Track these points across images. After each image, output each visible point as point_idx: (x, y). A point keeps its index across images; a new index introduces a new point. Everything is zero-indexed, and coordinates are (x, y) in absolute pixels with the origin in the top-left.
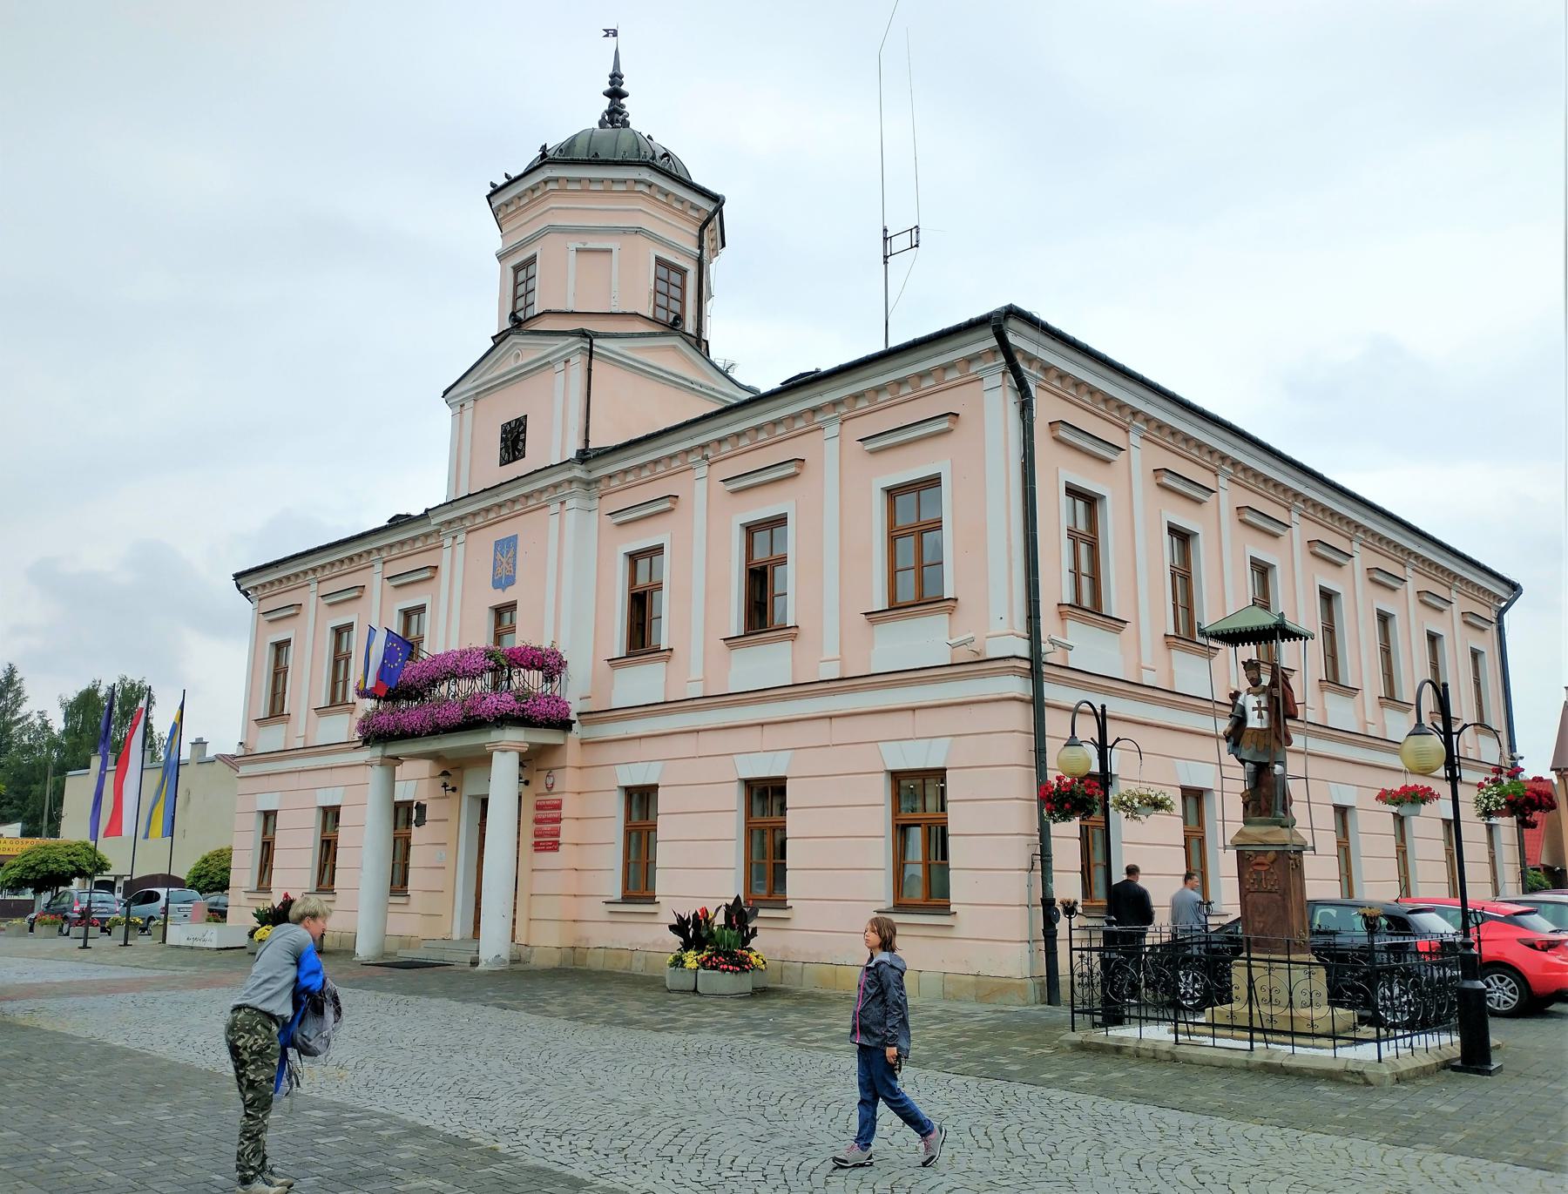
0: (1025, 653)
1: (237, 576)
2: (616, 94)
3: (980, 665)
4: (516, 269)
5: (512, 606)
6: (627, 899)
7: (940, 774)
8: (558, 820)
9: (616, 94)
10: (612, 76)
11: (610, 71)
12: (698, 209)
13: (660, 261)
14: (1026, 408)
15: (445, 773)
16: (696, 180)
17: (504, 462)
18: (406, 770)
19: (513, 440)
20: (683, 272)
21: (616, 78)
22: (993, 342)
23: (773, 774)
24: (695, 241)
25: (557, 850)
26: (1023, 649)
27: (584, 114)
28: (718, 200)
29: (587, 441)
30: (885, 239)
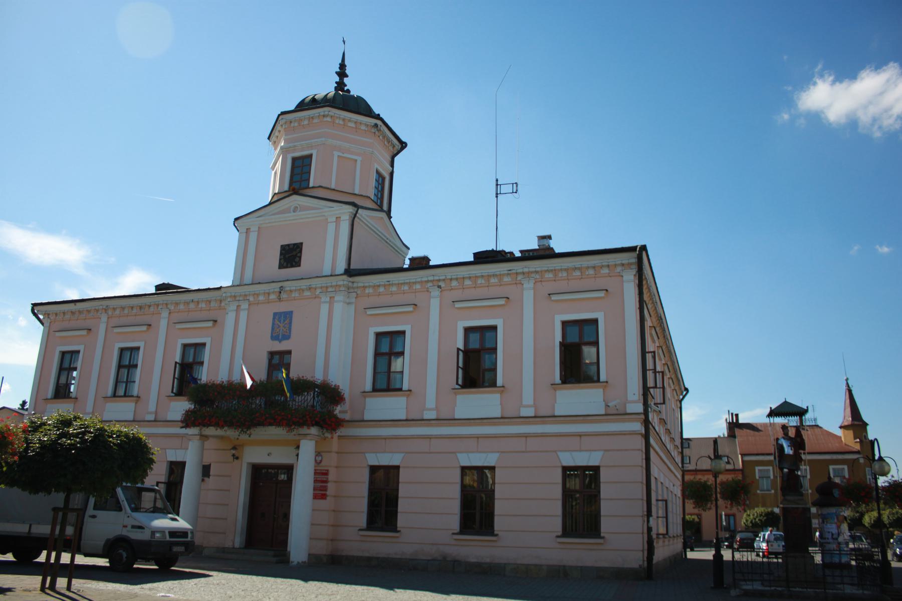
1: (34, 305)
3: (622, 415)
4: (294, 160)
8: (326, 482)
11: (340, 61)
15: (234, 448)
17: (281, 266)
18: (209, 444)
19: (291, 255)
21: (343, 66)
22: (634, 260)
25: (325, 499)
26: (640, 408)
30: (497, 185)
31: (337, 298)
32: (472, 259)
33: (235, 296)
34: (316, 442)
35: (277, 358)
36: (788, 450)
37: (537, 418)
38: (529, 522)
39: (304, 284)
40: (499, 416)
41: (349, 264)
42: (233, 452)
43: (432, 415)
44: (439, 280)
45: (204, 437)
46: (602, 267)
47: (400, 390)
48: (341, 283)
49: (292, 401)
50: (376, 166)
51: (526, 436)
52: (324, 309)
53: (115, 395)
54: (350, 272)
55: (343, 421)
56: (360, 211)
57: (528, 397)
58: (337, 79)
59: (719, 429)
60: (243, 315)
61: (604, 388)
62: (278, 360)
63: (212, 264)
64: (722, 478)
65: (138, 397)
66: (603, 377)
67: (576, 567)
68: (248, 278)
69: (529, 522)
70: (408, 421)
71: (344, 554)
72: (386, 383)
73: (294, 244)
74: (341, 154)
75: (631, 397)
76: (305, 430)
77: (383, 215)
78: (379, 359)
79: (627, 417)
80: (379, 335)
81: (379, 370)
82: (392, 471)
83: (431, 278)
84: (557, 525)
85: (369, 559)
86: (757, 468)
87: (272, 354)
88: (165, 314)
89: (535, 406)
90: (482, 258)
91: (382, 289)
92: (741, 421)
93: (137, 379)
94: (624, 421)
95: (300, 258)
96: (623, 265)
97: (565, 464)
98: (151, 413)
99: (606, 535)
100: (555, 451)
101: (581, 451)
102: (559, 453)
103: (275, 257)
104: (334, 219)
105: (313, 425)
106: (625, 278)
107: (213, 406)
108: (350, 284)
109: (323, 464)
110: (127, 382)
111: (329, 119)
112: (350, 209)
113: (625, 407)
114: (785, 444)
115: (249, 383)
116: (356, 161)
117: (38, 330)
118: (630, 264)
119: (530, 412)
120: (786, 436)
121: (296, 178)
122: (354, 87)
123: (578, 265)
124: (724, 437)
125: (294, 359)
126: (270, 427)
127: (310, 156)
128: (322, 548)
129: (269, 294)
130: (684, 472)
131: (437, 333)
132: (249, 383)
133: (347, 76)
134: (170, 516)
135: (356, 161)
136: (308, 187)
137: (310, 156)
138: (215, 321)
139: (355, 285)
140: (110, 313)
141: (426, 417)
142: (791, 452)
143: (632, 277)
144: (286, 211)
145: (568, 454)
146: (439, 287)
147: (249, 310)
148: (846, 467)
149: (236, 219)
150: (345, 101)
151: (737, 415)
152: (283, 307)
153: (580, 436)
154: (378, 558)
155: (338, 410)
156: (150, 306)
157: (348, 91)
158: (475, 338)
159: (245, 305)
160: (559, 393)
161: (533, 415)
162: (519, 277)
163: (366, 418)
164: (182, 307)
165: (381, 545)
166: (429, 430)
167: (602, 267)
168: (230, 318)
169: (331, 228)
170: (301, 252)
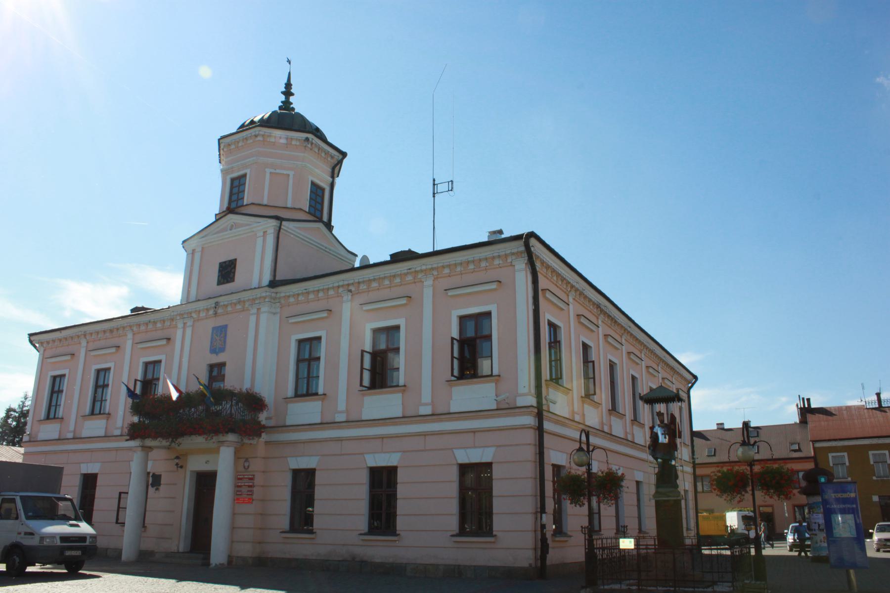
0: (535, 405)
1: (31, 335)
2: (288, 93)
4: (233, 180)
5: (222, 365)
6: (293, 529)
7: (489, 465)
9: (288, 93)
10: (286, 84)
11: (286, 81)
12: (332, 157)
13: (313, 183)
14: (535, 281)
15: (177, 458)
16: (329, 140)
17: (220, 283)
18: (153, 454)
19: (227, 271)
20: (323, 190)
21: (288, 85)
22: (523, 248)
23: (389, 464)
24: (330, 174)
26: (533, 401)
27: (271, 104)
28: (344, 155)
29: (275, 276)
30: (434, 185)
31: (263, 309)
32: (388, 259)
33: (182, 315)
34: (236, 448)
35: (216, 370)
36: (663, 439)
37: (435, 416)
38: (428, 523)
39: (234, 298)
40: (401, 415)
41: (275, 276)
42: (177, 461)
43: (341, 418)
44: (348, 285)
45: (147, 449)
46: (493, 258)
47: (316, 394)
48: (264, 294)
49: (220, 411)
50: (311, 178)
51: (425, 434)
52: (253, 319)
53: (92, 413)
54: (273, 284)
55: (264, 427)
56: (284, 223)
57: (426, 397)
58: (283, 98)
59: (792, 416)
60: (189, 331)
61: (497, 382)
62: (216, 371)
63: (167, 287)
64: (757, 468)
65: (109, 414)
66: (495, 372)
67: (470, 567)
68: (193, 297)
69: (428, 523)
70: (323, 425)
71: (270, 556)
72: (306, 390)
73: (230, 261)
74: (273, 171)
75: (522, 390)
76: (222, 438)
77: (320, 226)
78: (301, 365)
79: (517, 410)
80: (300, 342)
81: (300, 376)
82: (310, 473)
83: (341, 283)
84: (453, 523)
85: (290, 560)
86: (830, 455)
87: (212, 367)
88: (130, 336)
89: (433, 403)
90: (398, 258)
91: (301, 298)
92: (813, 406)
93: (108, 398)
94: (514, 415)
95: (234, 273)
96: (513, 254)
97: (460, 462)
98: (117, 428)
99: (401, 533)
100: (452, 449)
101: (475, 447)
102: (455, 451)
103: (214, 273)
104: (262, 234)
105: (227, 433)
106: (517, 267)
107: (157, 418)
108: (273, 295)
109: (250, 469)
110: (102, 401)
111: (260, 138)
112: (274, 223)
113: (515, 401)
114: (659, 431)
115: (175, 395)
116: (288, 175)
117: (33, 356)
118: (521, 252)
119: (426, 410)
120: (662, 425)
121: (234, 197)
122: (299, 105)
123: (470, 258)
124: (796, 424)
125: (228, 371)
126: (193, 437)
127: (245, 176)
128: (246, 550)
129: (199, 311)
130: (695, 466)
131: (348, 338)
132: (175, 395)
133: (292, 94)
134: (71, 522)
135: (288, 175)
136: (243, 206)
137: (245, 176)
138: (169, 339)
139: (278, 295)
140: (88, 337)
141: (337, 420)
142: (666, 441)
143: (524, 265)
144: (225, 230)
145: (462, 451)
146: (350, 291)
147: (193, 326)
148: (846, 454)
149: (184, 242)
150: (286, 119)
151: (808, 400)
152: (220, 322)
153: (474, 432)
154: (297, 560)
155: (262, 417)
156: (118, 329)
157: (293, 109)
158: (383, 338)
159: (190, 323)
160: (454, 389)
161: (430, 413)
162: (420, 276)
163: (287, 424)
164: (143, 328)
165: (301, 547)
166: (343, 433)
167: (493, 258)
168: (179, 333)
169: (260, 241)
170: (235, 267)
